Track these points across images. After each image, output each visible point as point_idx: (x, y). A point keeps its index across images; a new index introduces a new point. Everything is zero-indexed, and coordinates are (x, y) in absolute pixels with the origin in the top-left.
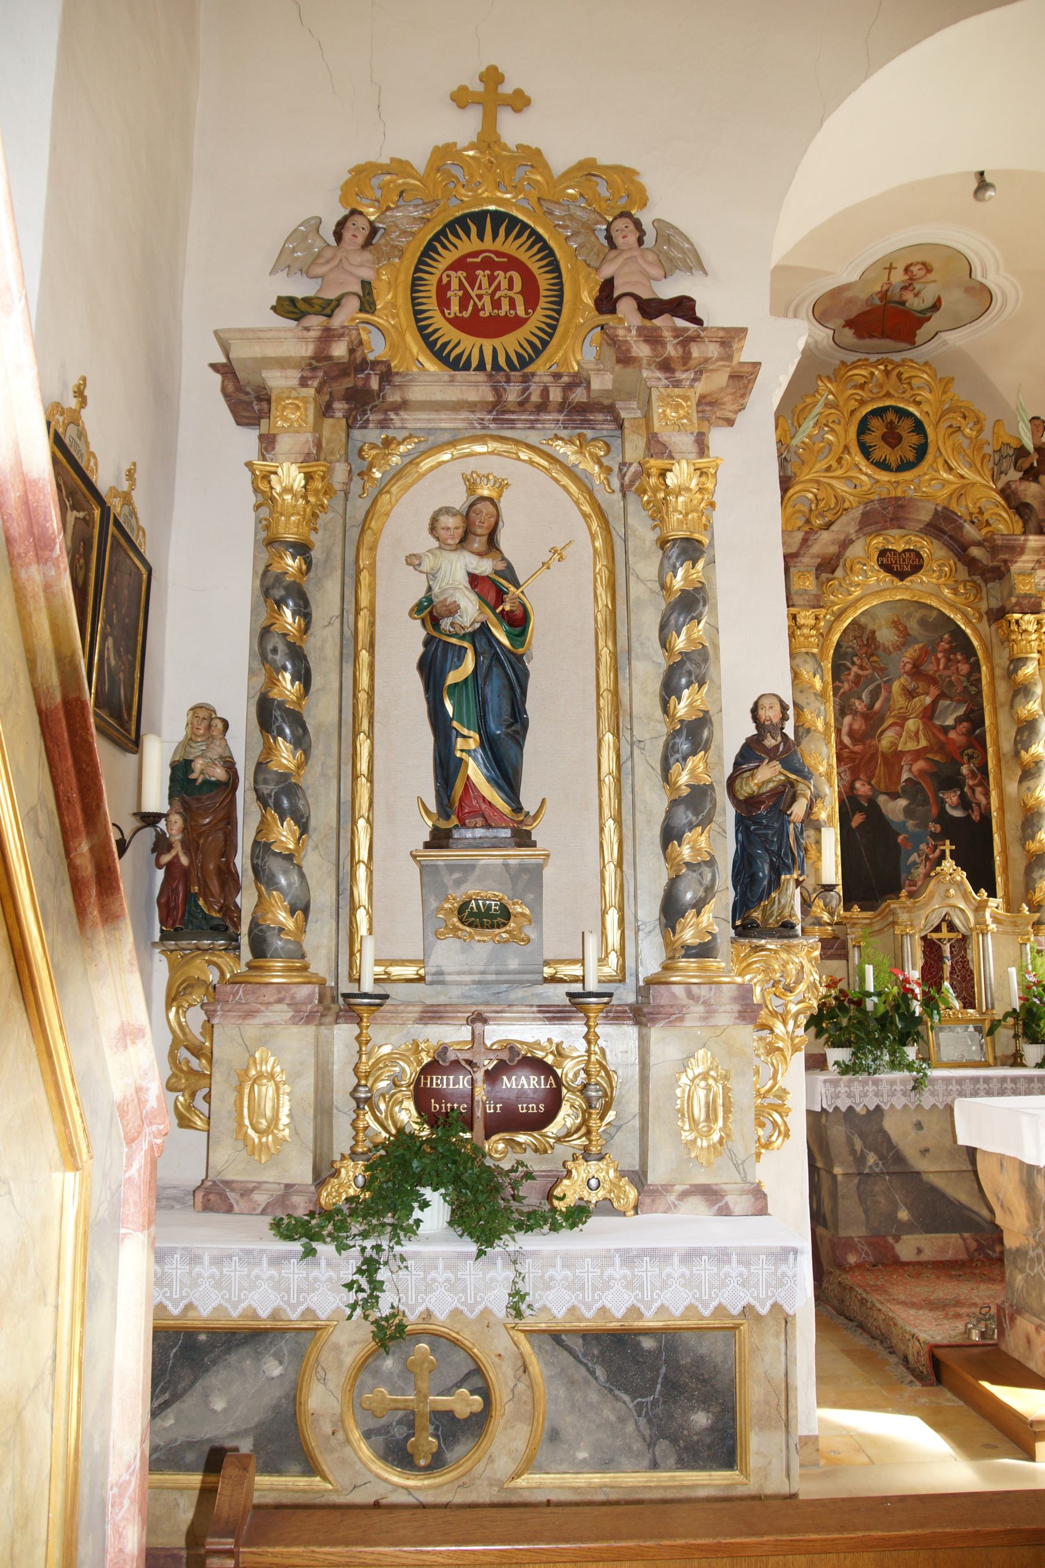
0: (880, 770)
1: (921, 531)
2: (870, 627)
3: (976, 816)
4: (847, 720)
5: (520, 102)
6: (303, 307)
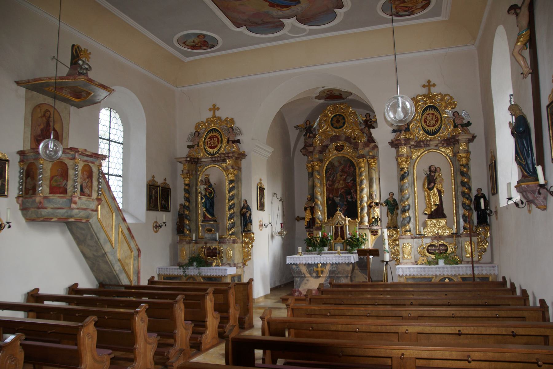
2: (333, 162)
3: (354, 200)
4: (328, 182)
5: (218, 109)
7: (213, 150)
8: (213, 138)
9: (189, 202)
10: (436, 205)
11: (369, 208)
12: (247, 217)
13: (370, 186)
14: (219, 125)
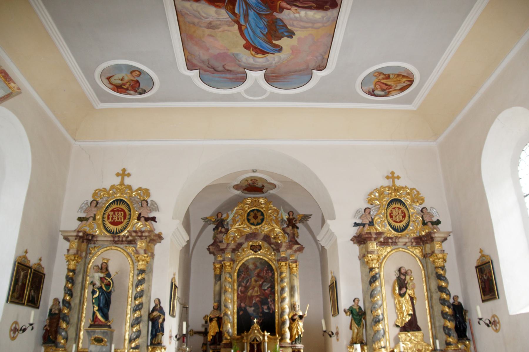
0: (248, 300)
1: (262, 240)
2: (247, 264)
3: (271, 312)
4: (240, 288)
5: (129, 175)
6: (82, 219)
7: (115, 227)
8: (118, 211)
9: (71, 295)
10: (409, 315)
11: (291, 321)
12: (158, 323)
13: (292, 296)
14: (128, 195)
